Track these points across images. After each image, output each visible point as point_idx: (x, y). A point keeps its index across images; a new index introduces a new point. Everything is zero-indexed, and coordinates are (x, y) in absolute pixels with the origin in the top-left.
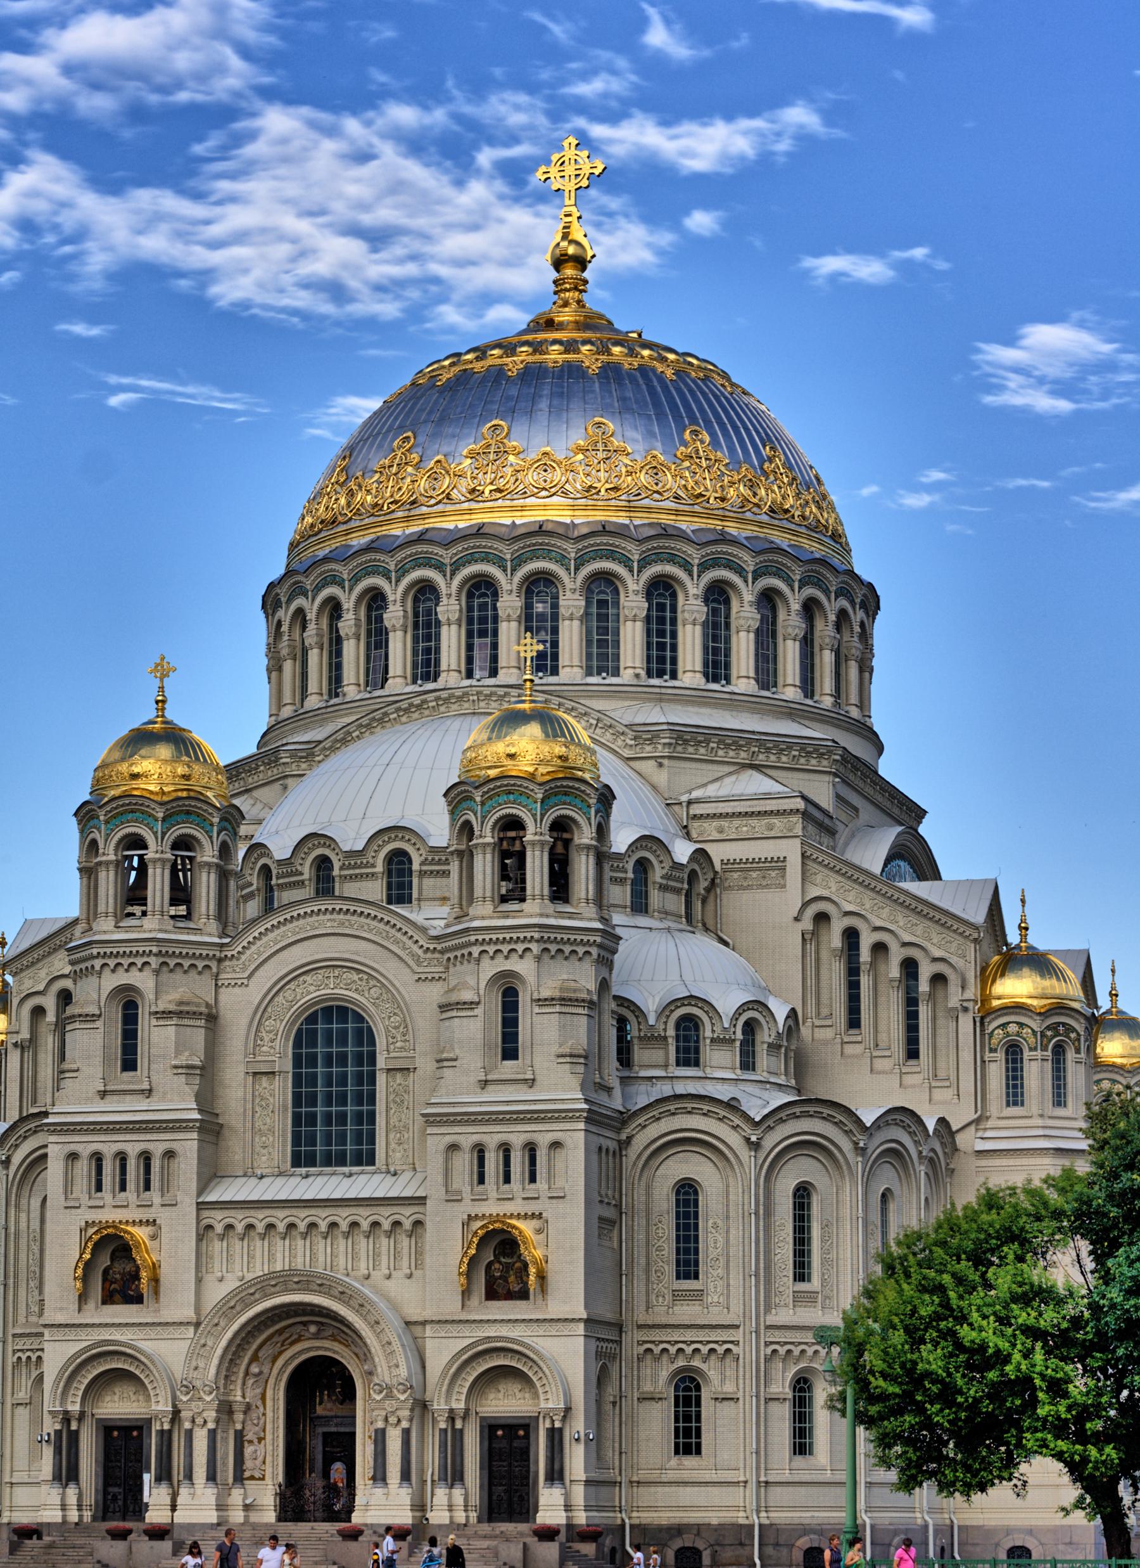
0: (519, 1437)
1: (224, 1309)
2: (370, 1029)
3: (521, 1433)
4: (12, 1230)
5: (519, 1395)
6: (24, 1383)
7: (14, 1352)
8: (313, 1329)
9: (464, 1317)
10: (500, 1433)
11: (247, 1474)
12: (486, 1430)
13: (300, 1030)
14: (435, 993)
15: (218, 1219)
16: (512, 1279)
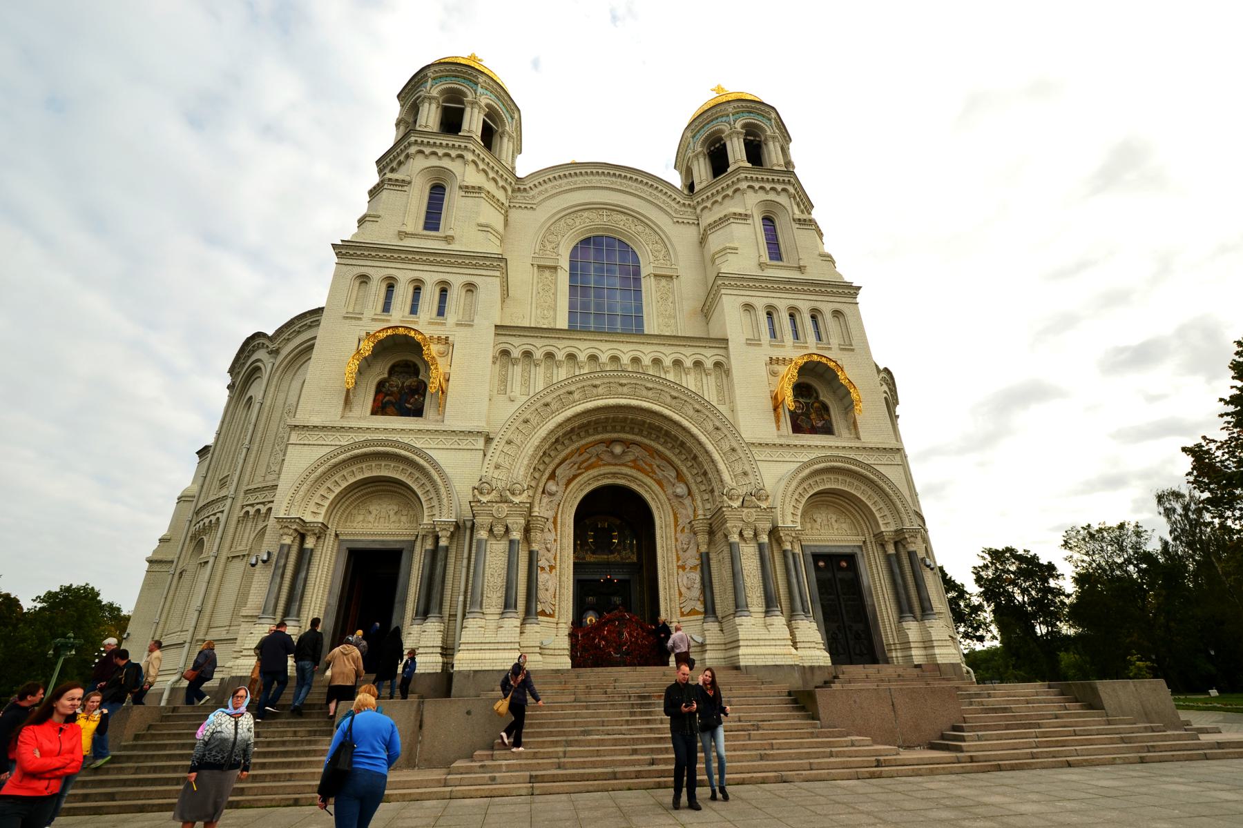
0: (842, 569)
1: (537, 405)
2: (634, 252)
3: (844, 564)
4: (268, 402)
5: (836, 526)
6: (246, 535)
7: (243, 507)
8: (618, 449)
9: (782, 441)
10: (821, 564)
11: (539, 608)
12: (810, 559)
13: (575, 247)
14: (691, 234)
15: (517, 346)
16: (813, 416)
